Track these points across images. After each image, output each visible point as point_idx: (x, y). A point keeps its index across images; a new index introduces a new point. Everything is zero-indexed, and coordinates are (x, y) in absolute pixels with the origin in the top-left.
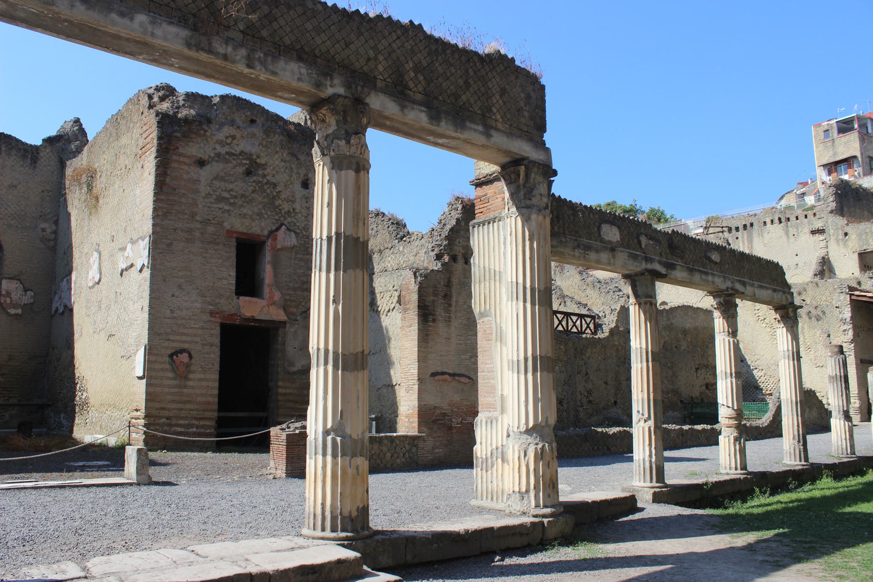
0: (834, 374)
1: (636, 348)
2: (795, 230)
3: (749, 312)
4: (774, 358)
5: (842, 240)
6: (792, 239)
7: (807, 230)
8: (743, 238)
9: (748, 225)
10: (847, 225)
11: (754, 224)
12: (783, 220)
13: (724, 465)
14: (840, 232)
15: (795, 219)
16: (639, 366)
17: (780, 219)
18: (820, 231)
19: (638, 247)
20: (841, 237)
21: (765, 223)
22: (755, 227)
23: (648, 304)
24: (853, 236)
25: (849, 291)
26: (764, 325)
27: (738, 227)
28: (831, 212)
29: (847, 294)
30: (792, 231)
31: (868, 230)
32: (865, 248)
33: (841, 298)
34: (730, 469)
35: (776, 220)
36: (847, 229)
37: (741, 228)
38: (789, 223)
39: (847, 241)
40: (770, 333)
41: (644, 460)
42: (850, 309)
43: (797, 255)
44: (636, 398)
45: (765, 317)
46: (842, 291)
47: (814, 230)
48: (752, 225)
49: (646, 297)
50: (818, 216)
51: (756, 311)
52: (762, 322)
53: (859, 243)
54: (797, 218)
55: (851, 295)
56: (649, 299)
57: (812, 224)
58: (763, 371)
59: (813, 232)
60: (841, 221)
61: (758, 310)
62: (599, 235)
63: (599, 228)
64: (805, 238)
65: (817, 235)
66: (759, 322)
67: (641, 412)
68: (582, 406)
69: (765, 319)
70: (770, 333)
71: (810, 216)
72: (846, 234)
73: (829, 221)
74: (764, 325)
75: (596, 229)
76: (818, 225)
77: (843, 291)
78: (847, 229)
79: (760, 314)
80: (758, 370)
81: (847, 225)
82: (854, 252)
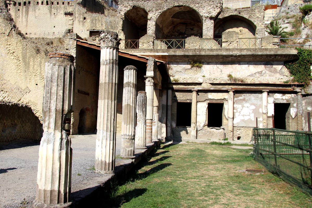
2: (56, 10)
3: (2, 46)
4: (17, 84)
5: (82, 21)
6: (53, 16)
7: (62, 12)
8: (22, 10)
9: (27, 2)
10: (86, 13)
11: (31, 2)
12: (49, 3)
14: (82, 16)
15: (56, 4)
17: (47, 2)
18: (70, 14)
20: (82, 19)
21: (38, 3)
22: (32, 4)
24: (88, 20)
25: (77, 38)
26: (12, 57)
27: (21, 3)
28: (79, 4)
29: (75, 40)
30: (54, 11)
31: (97, 18)
32: (94, 28)
33: (71, 43)
35: (45, 3)
36: (86, 15)
37: (22, 3)
38: (53, 6)
39: (84, 22)
40: (16, 64)
42: (75, 52)
43: (54, 27)
45: (14, 51)
46: (72, 37)
47: (67, 12)
48: (29, 3)
50: (70, 4)
51: (8, 46)
52: (12, 54)
53: (91, 25)
54: (58, 3)
55: (77, 41)
57: (66, 9)
58: (7, 93)
59: (66, 14)
60: (84, 10)
61: (10, 45)
64: (61, 17)
65: (68, 16)
66: (9, 54)
69: (14, 52)
70: (16, 64)
71: (66, 4)
72: (85, 18)
73: (76, 9)
74: (12, 57)
76: (70, 10)
77: (72, 37)
78: (86, 15)
79: (10, 49)
80: (3, 92)
81: (86, 13)
82: (87, 30)
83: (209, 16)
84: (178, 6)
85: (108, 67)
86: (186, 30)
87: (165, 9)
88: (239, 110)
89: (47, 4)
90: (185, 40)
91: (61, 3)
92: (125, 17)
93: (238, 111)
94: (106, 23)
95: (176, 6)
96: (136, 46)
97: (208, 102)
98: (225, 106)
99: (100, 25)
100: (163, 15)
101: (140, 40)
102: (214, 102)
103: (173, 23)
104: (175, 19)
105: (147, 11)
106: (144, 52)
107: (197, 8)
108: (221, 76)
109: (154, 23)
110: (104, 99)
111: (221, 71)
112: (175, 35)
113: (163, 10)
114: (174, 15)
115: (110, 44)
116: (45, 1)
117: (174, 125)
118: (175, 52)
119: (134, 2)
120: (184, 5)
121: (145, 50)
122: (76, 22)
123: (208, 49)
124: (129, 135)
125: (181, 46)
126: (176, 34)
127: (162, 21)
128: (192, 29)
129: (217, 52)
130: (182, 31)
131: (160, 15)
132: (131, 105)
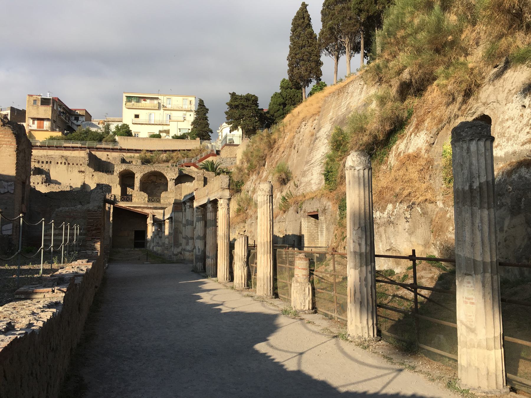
6: (69, 173)
24: (96, 177)
36: (94, 174)
54: (73, 164)
59: (79, 172)
60: (92, 170)
72: (93, 175)
76: (83, 169)
83: (173, 178)
89: (65, 164)
91: (75, 164)
94: (108, 179)
100: (144, 175)
109: (139, 180)
116: (64, 162)
122: (87, 178)
128: (161, 180)
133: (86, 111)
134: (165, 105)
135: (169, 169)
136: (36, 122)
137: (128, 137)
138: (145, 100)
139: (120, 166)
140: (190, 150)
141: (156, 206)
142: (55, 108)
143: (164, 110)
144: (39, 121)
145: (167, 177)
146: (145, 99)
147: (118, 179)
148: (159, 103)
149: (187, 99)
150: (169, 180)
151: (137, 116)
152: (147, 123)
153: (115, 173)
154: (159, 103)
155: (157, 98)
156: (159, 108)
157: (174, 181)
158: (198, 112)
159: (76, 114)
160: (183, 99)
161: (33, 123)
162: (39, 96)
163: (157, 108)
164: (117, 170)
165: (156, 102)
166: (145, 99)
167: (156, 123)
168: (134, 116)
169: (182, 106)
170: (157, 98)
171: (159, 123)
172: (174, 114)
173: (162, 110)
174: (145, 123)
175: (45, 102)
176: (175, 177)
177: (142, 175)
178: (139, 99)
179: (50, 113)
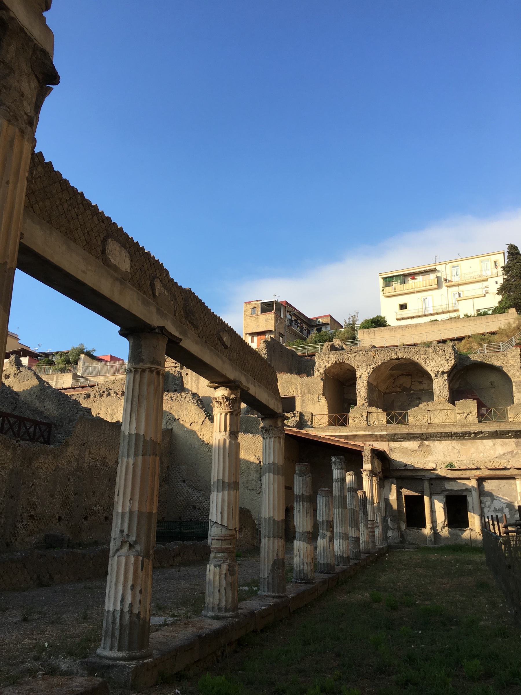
0: (300, 494)
1: (130, 435)
13: (211, 605)
16: (131, 461)
19: (151, 292)
23: (155, 373)
34: (220, 609)
41: (122, 610)
44: (120, 510)
49: (152, 363)
56: (156, 367)
62: (103, 252)
63: (104, 241)
67: (126, 532)
68: (23, 521)
74: (207, 450)
75: (99, 243)
83: (441, 369)
84: (397, 359)
85: (339, 483)
86: (412, 384)
87: (380, 364)
88: (488, 504)
90: (407, 412)
92: (326, 375)
93: (487, 506)
94: (302, 385)
95: (393, 359)
96: (343, 422)
97: (446, 493)
98: (469, 499)
99: (294, 389)
100: (376, 370)
101: (349, 414)
102: (453, 494)
103: (392, 375)
104: (394, 371)
105: (355, 367)
106: (356, 432)
107: (422, 361)
108: (459, 459)
109: (365, 382)
110: (339, 508)
111: (459, 452)
112: (396, 392)
113: (377, 365)
114: (392, 368)
115: (340, 467)
117: (404, 526)
118: (395, 429)
119: (336, 355)
120: (404, 357)
121: (358, 428)
123: (438, 425)
124: (354, 537)
125: (403, 420)
126: (398, 390)
127: (375, 377)
128: (421, 383)
129: (449, 429)
130: (406, 386)
131: (373, 371)
132: (355, 509)
133: (331, 317)
134: (449, 278)
135: (430, 350)
136: (256, 339)
137: (376, 329)
138: (412, 279)
139: (325, 358)
140: (493, 333)
141: (393, 432)
142: (282, 316)
143: (448, 286)
144: (259, 337)
145: (428, 369)
146: (413, 275)
147: (321, 384)
148: (438, 278)
149: (488, 260)
150: (433, 375)
151: (403, 307)
152: (421, 314)
153: (316, 374)
154: (438, 278)
155: (434, 271)
156: (439, 286)
157: (445, 376)
158: (509, 267)
159: (318, 323)
160: (482, 261)
161: (252, 341)
162: (259, 301)
163: (436, 286)
164: (320, 367)
165: (432, 277)
166: (413, 275)
167: (436, 311)
168: (398, 307)
169: (480, 274)
170: (434, 271)
171: (441, 311)
172: (467, 290)
173: (444, 288)
174: (417, 314)
175: (266, 307)
176: (447, 367)
177: (370, 369)
178: (403, 278)
179: (273, 322)
